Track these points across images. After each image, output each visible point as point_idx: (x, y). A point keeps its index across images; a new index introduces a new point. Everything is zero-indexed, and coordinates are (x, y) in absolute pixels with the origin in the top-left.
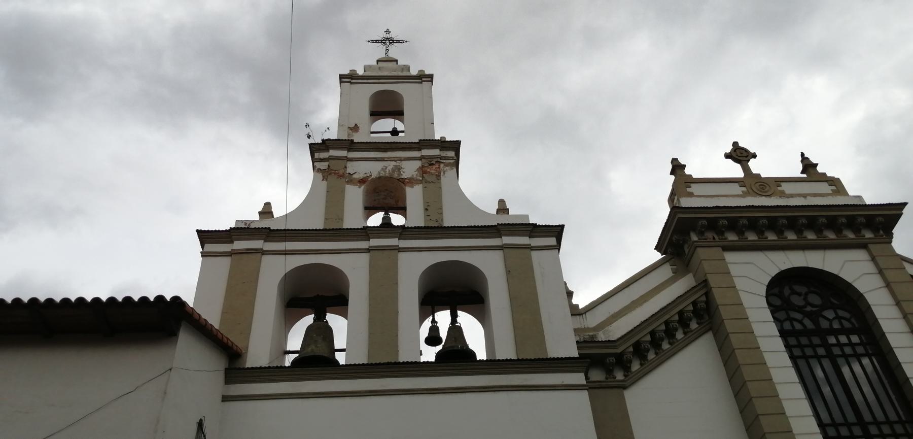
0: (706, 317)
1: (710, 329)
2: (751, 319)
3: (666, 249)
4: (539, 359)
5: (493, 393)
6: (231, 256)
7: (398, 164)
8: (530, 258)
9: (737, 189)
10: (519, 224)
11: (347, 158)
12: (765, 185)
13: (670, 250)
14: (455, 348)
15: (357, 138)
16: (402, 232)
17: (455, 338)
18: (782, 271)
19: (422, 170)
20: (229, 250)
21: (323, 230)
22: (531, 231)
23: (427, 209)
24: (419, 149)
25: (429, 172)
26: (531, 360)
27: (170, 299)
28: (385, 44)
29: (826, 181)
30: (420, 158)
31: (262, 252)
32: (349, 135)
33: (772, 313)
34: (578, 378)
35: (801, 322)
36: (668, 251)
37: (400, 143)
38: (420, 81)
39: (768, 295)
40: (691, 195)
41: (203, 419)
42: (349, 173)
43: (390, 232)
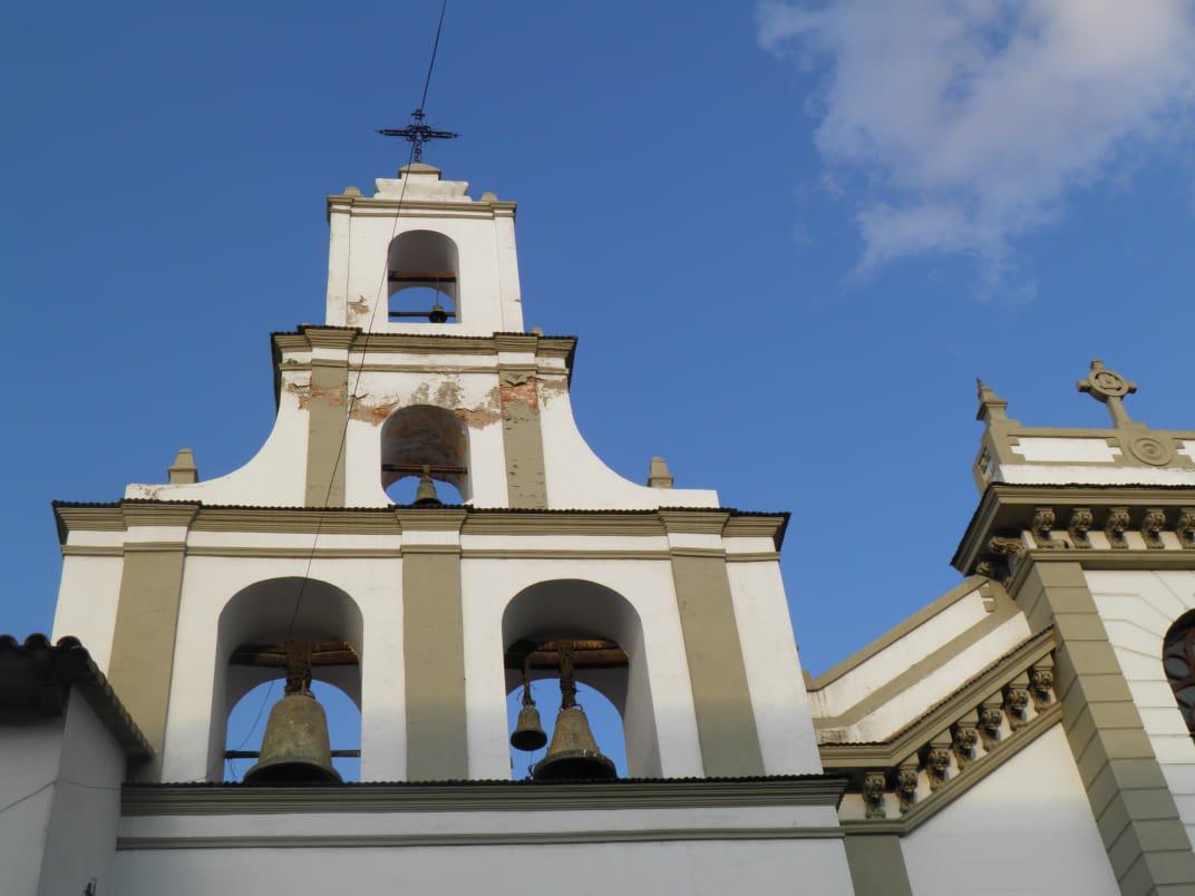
1: (1060, 721)
2: (1138, 702)
3: (975, 564)
4: (749, 779)
5: (659, 843)
7: (450, 381)
8: (723, 580)
10: (701, 510)
12: (1155, 444)
14: (576, 755)
15: (365, 323)
16: (467, 518)
17: (574, 735)
19: (501, 395)
20: (119, 544)
21: (307, 509)
22: (725, 524)
23: (511, 474)
24: (495, 352)
25: (515, 399)
26: (733, 780)
27: (58, 643)
28: (413, 138)
31: (186, 550)
32: (349, 318)
33: (1175, 690)
36: (979, 567)
38: (491, 214)
39: (1169, 655)
40: (1020, 460)
41: (93, 883)
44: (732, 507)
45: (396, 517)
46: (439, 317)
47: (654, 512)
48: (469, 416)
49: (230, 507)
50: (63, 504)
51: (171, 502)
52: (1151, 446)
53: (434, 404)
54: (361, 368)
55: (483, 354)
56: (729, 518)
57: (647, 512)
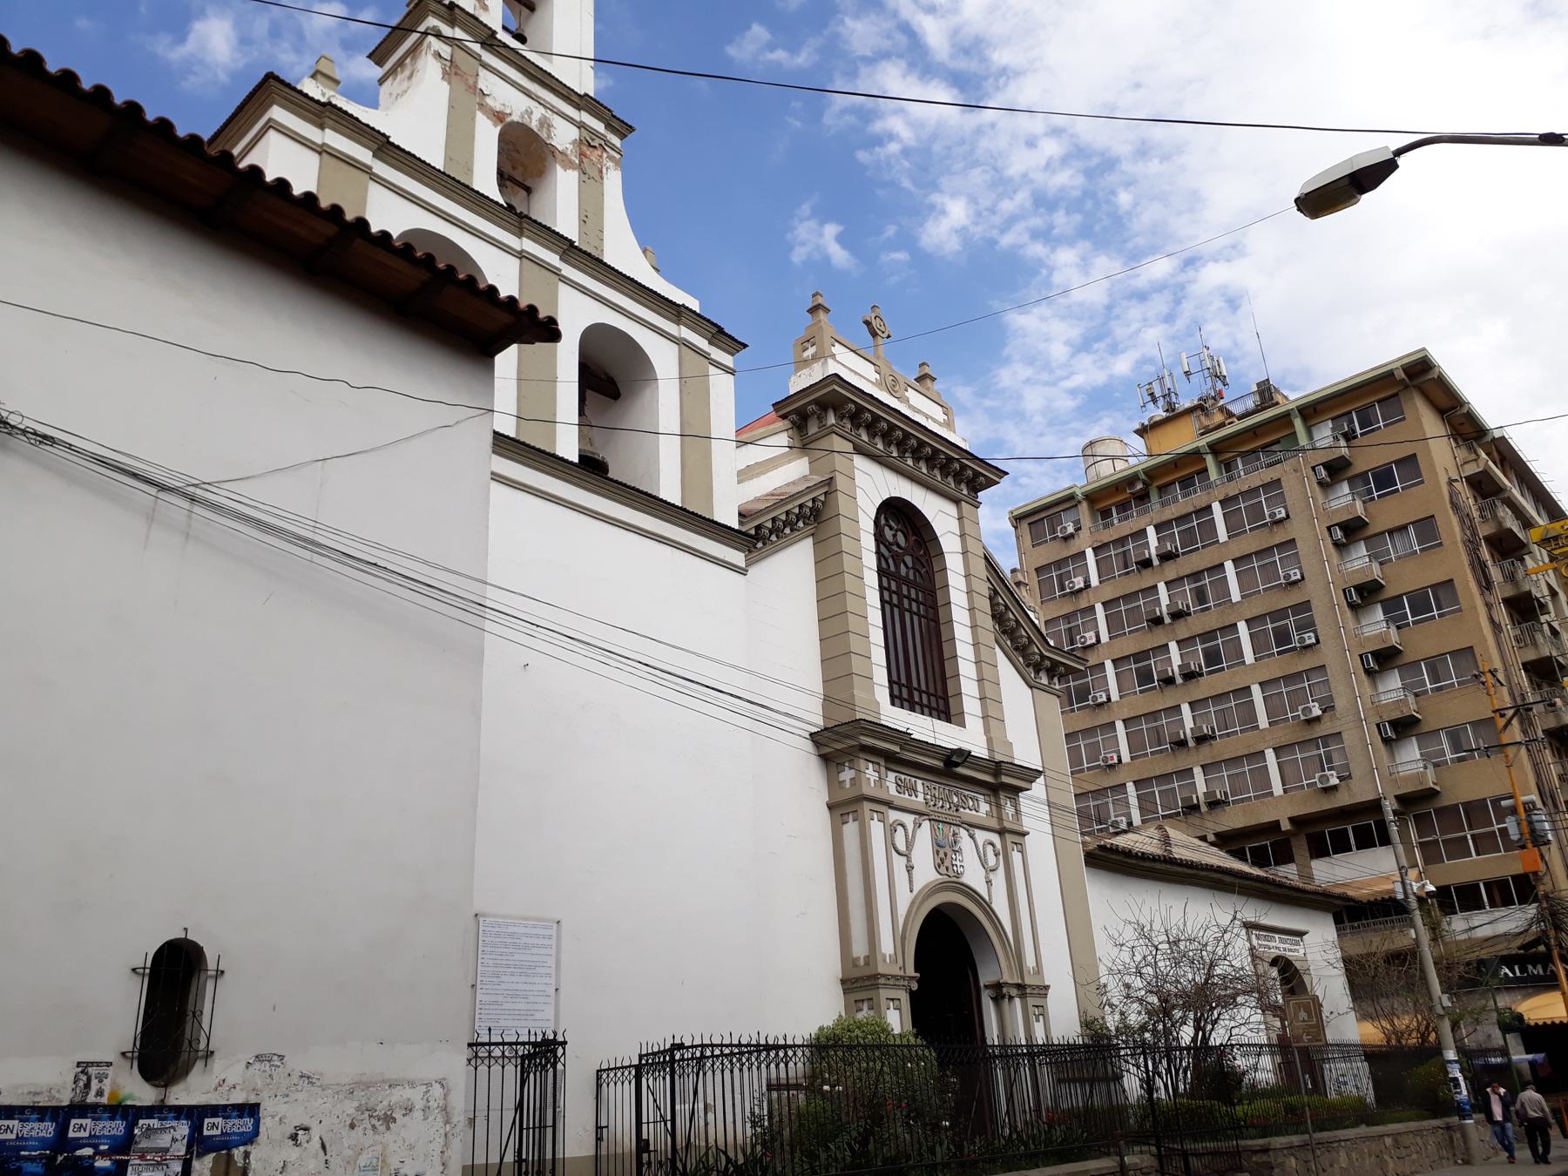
0: (812, 518)
5: (657, 543)
6: (320, 153)
9: (868, 370)
11: (480, 60)
13: (794, 416)
14: (596, 457)
20: (319, 142)
23: (585, 222)
24: (578, 108)
29: (942, 406)
30: (581, 126)
34: (738, 557)
37: (557, 80)
39: (877, 522)
45: (520, 223)
46: (521, 38)
47: (679, 305)
50: (277, 79)
51: (367, 126)
53: (535, 130)
54: (486, 66)
56: (719, 335)
57: (674, 304)
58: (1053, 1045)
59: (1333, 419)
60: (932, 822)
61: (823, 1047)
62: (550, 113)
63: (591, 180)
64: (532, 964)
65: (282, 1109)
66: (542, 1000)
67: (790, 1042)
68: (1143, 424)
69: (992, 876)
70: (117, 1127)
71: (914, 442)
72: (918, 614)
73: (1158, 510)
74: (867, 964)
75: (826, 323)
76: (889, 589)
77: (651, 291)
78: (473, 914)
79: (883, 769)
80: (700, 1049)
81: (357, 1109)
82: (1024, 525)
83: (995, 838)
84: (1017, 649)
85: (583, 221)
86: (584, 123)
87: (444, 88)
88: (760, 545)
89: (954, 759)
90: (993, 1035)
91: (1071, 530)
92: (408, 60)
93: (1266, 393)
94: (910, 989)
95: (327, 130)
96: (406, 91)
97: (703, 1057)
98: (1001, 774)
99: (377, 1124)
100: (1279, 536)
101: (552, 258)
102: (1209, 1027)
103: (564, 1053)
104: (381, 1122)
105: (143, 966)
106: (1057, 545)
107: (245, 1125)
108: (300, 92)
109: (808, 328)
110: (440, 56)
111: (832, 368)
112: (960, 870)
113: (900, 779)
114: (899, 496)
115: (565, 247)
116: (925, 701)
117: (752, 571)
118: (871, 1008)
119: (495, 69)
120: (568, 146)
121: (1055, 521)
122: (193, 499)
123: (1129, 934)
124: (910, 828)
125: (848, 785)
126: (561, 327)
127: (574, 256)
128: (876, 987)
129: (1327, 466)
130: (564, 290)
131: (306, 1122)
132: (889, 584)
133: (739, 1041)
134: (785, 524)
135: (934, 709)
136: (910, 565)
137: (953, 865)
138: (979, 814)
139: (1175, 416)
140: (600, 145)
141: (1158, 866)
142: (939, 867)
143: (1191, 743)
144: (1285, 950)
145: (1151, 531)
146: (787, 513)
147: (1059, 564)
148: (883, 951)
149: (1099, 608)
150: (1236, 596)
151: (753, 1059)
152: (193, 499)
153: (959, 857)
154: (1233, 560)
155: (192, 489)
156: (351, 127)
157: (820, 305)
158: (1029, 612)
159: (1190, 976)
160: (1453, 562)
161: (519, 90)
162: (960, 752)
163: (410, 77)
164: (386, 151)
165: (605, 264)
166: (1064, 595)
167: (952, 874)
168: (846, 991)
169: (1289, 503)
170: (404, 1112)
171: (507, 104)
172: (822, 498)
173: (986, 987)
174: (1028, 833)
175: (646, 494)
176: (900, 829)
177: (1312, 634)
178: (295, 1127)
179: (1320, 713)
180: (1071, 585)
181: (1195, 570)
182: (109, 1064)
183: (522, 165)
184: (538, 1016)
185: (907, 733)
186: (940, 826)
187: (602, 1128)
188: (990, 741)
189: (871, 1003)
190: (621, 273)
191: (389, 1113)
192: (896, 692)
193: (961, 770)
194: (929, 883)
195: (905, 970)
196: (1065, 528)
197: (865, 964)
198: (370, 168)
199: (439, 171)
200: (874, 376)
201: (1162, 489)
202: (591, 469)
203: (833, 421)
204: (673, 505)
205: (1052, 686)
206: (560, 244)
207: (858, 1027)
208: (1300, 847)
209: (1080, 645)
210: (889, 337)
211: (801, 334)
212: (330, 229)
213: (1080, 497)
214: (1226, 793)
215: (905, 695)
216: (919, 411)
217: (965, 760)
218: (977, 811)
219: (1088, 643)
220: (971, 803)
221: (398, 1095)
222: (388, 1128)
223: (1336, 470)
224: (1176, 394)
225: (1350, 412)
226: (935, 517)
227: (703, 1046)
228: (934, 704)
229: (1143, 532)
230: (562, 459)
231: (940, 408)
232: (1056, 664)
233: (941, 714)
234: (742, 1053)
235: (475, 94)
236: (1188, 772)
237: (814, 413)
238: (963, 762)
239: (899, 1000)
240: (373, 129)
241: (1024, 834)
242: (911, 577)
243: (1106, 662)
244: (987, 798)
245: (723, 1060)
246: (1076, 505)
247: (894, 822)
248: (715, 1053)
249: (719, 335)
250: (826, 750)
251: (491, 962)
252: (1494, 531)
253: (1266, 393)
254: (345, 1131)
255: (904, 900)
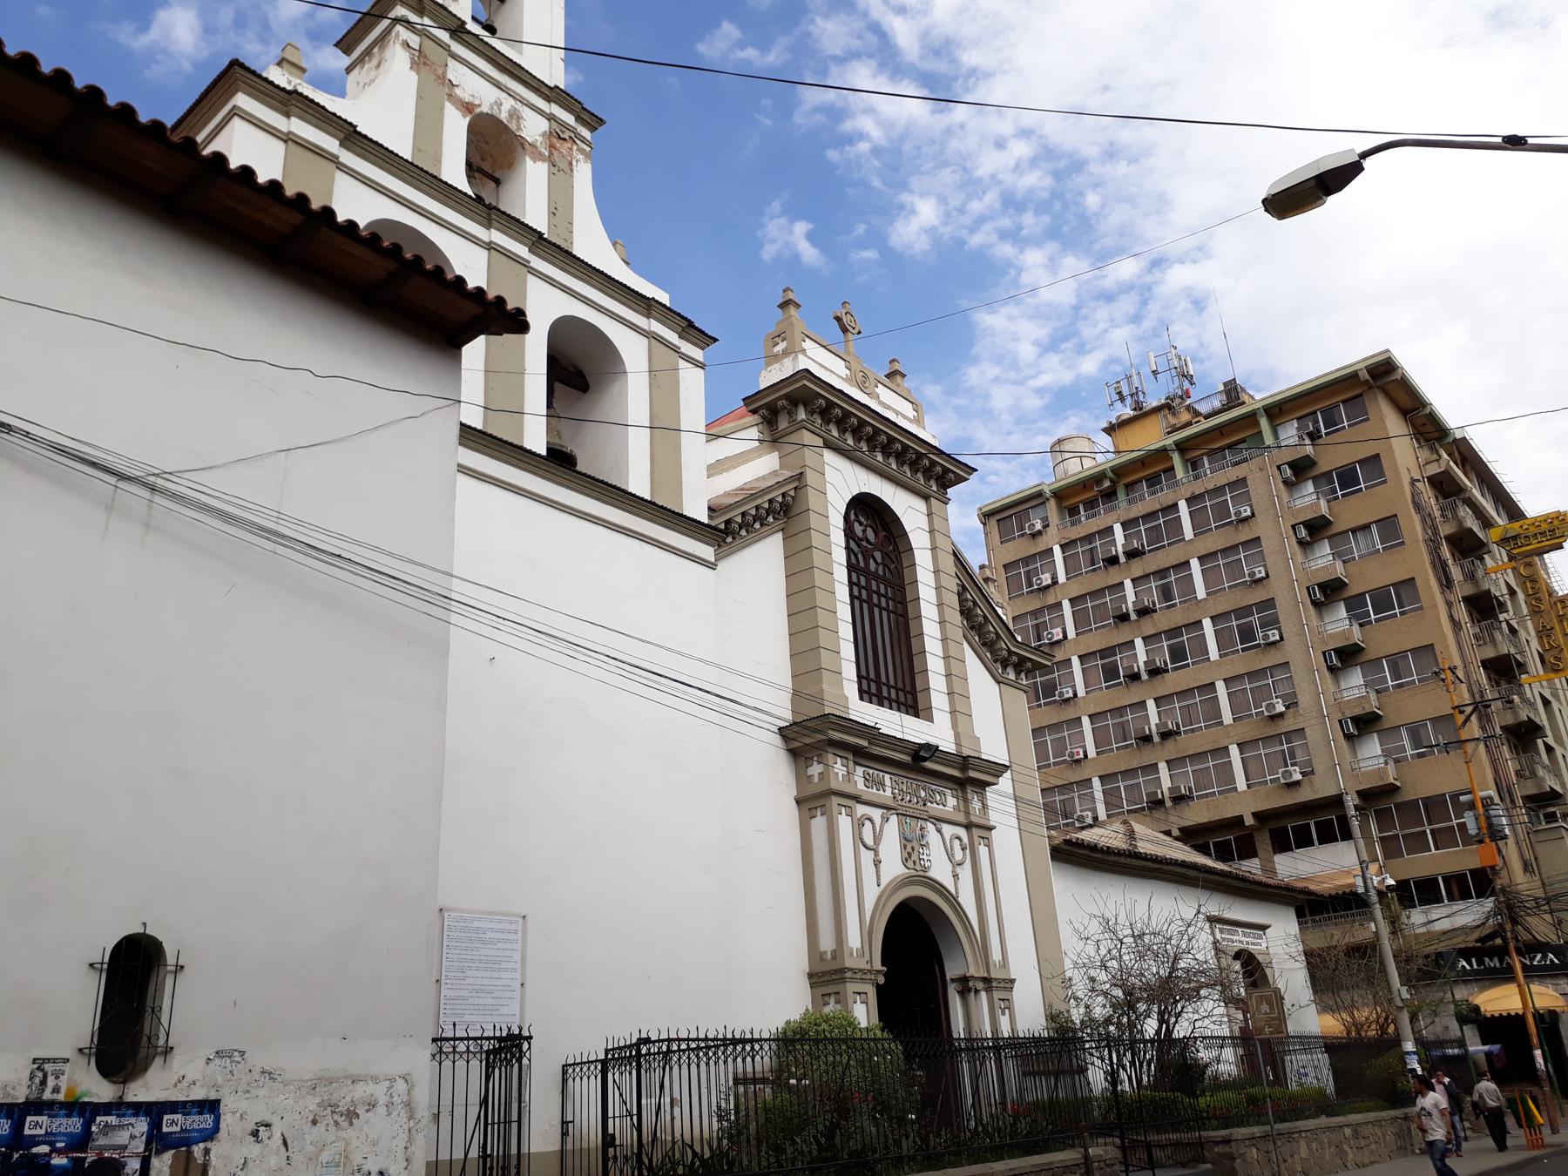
0: (782, 513)
1: (782, 530)
3: (760, 407)
6: (285, 142)
9: (839, 366)
11: (449, 51)
14: (564, 450)
18: (861, 493)
23: (554, 214)
24: (548, 100)
25: (561, 152)
29: (912, 403)
30: (551, 118)
34: (707, 552)
35: (856, 555)
37: (527, 71)
39: (846, 518)
42: (450, 81)
43: (520, 231)
44: (692, 320)
45: (489, 214)
46: (491, 30)
47: (648, 299)
48: (527, 146)
49: (376, 143)
50: (242, 66)
51: (334, 114)
52: (865, 376)
53: (505, 121)
54: (455, 57)
55: (540, 96)
56: (689, 329)
57: (644, 297)
58: (1019, 1038)
59: (1298, 419)
60: (900, 816)
61: (789, 1041)
62: (520, 104)
63: (560, 172)
64: (498, 959)
65: (244, 1105)
66: (508, 994)
67: (756, 1036)
68: (1111, 423)
69: (958, 870)
70: (74, 1124)
71: (883, 438)
72: (887, 609)
73: (1126, 508)
74: (834, 957)
75: (796, 318)
76: (858, 585)
77: (621, 283)
78: (438, 909)
79: (851, 764)
80: (666, 1043)
81: (319, 1105)
82: (993, 522)
83: (962, 832)
84: (984, 644)
85: (553, 213)
86: (554, 115)
87: (413, 77)
88: (729, 539)
89: (922, 753)
90: (959, 1028)
91: (1038, 526)
92: (376, 50)
93: (1233, 392)
94: (877, 983)
95: (293, 119)
96: (374, 80)
97: (669, 1051)
98: (968, 768)
99: (340, 1120)
100: (1245, 534)
101: (521, 250)
102: (1173, 1020)
103: (529, 1048)
104: (344, 1118)
105: (100, 961)
106: (1025, 542)
107: (206, 1121)
108: (266, 80)
109: (777, 324)
110: (408, 45)
111: (803, 363)
112: (927, 864)
113: (868, 774)
114: (869, 491)
115: (534, 239)
116: (893, 696)
117: (722, 565)
118: (837, 1002)
119: (464, 59)
120: (538, 138)
121: (1023, 517)
122: (153, 489)
123: (1094, 928)
124: (878, 822)
125: (816, 780)
126: (529, 319)
127: (541, 247)
128: (843, 981)
129: (1292, 465)
130: (531, 280)
131: (267, 1118)
132: (859, 579)
133: (706, 1036)
134: (755, 518)
135: (903, 704)
136: (879, 561)
137: (920, 859)
138: (946, 808)
139: (1142, 415)
140: (570, 137)
141: (1122, 860)
142: (906, 860)
143: (1156, 739)
144: (1248, 943)
145: (1118, 529)
146: (757, 508)
147: (1027, 560)
148: (850, 945)
149: (1066, 604)
150: (1201, 593)
151: (720, 1053)
152: (153, 489)
153: (926, 852)
154: (1199, 558)
155: (152, 479)
156: (317, 115)
157: (790, 300)
158: (997, 608)
159: (1154, 969)
160: (1415, 561)
161: (487, 80)
162: (928, 746)
163: (378, 66)
164: (352, 139)
165: (575, 256)
166: (1032, 592)
167: (918, 868)
168: (812, 985)
169: (1254, 501)
170: (367, 1108)
171: (476, 95)
172: (792, 493)
173: (952, 980)
174: (995, 828)
175: (614, 487)
176: (867, 823)
177: (1276, 631)
178: (257, 1123)
179: (1283, 709)
180: (1039, 582)
181: (1161, 568)
182: (66, 1061)
183: (491, 156)
184: (503, 1010)
185: (875, 728)
186: (908, 821)
187: (567, 1123)
188: (957, 736)
189: (837, 996)
190: (590, 266)
191: (352, 1109)
192: (865, 687)
193: (928, 765)
194: (895, 878)
195: (871, 964)
196: (1033, 525)
197: (832, 959)
198: (337, 157)
199: (407, 161)
200: (844, 372)
201: (1129, 487)
202: (559, 462)
203: (804, 417)
204: (642, 499)
205: (1020, 681)
206: (529, 237)
207: (825, 1021)
208: (1263, 842)
209: (1047, 642)
210: (859, 333)
211: (773, 329)
212: (295, 218)
213: (1048, 494)
214: (1190, 788)
215: (874, 690)
216: (889, 408)
217: (932, 755)
218: (944, 806)
219: (1055, 639)
220: (938, 798)
221: (361, 1091)
222: (351, 1124)
223: (1301, 469)
224: (1144, 393)
225: (1315, 412)
226: (904, 513)
227: (669, 1040)
228: (902, 700)
229: (1110, 530)
230: (530, 452)
231: (911, 404)
232: (1023, 660)
233: (910, 709)
234: (708, 1047)
235: (443, 84)
236: (1154, 768)
237: (784, 408)
238: (931, 757)
239: (866, 993)
240: (340, 118)
241: (990, 829)
242: (881, 573)
243: (1072, 658)
244: (954, 792)
245: (689, 1055)
246: (1044, 503)
247: (863, 816)
248: (682, 1048)
249: (689, 329)
250: (795, 745)
251: (455, 957)
252: (1454, 530)
253: (1233, 392)
254: (307, 1128)
255: (871, 894)
